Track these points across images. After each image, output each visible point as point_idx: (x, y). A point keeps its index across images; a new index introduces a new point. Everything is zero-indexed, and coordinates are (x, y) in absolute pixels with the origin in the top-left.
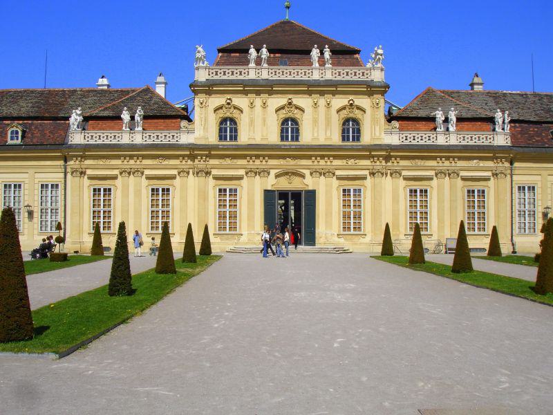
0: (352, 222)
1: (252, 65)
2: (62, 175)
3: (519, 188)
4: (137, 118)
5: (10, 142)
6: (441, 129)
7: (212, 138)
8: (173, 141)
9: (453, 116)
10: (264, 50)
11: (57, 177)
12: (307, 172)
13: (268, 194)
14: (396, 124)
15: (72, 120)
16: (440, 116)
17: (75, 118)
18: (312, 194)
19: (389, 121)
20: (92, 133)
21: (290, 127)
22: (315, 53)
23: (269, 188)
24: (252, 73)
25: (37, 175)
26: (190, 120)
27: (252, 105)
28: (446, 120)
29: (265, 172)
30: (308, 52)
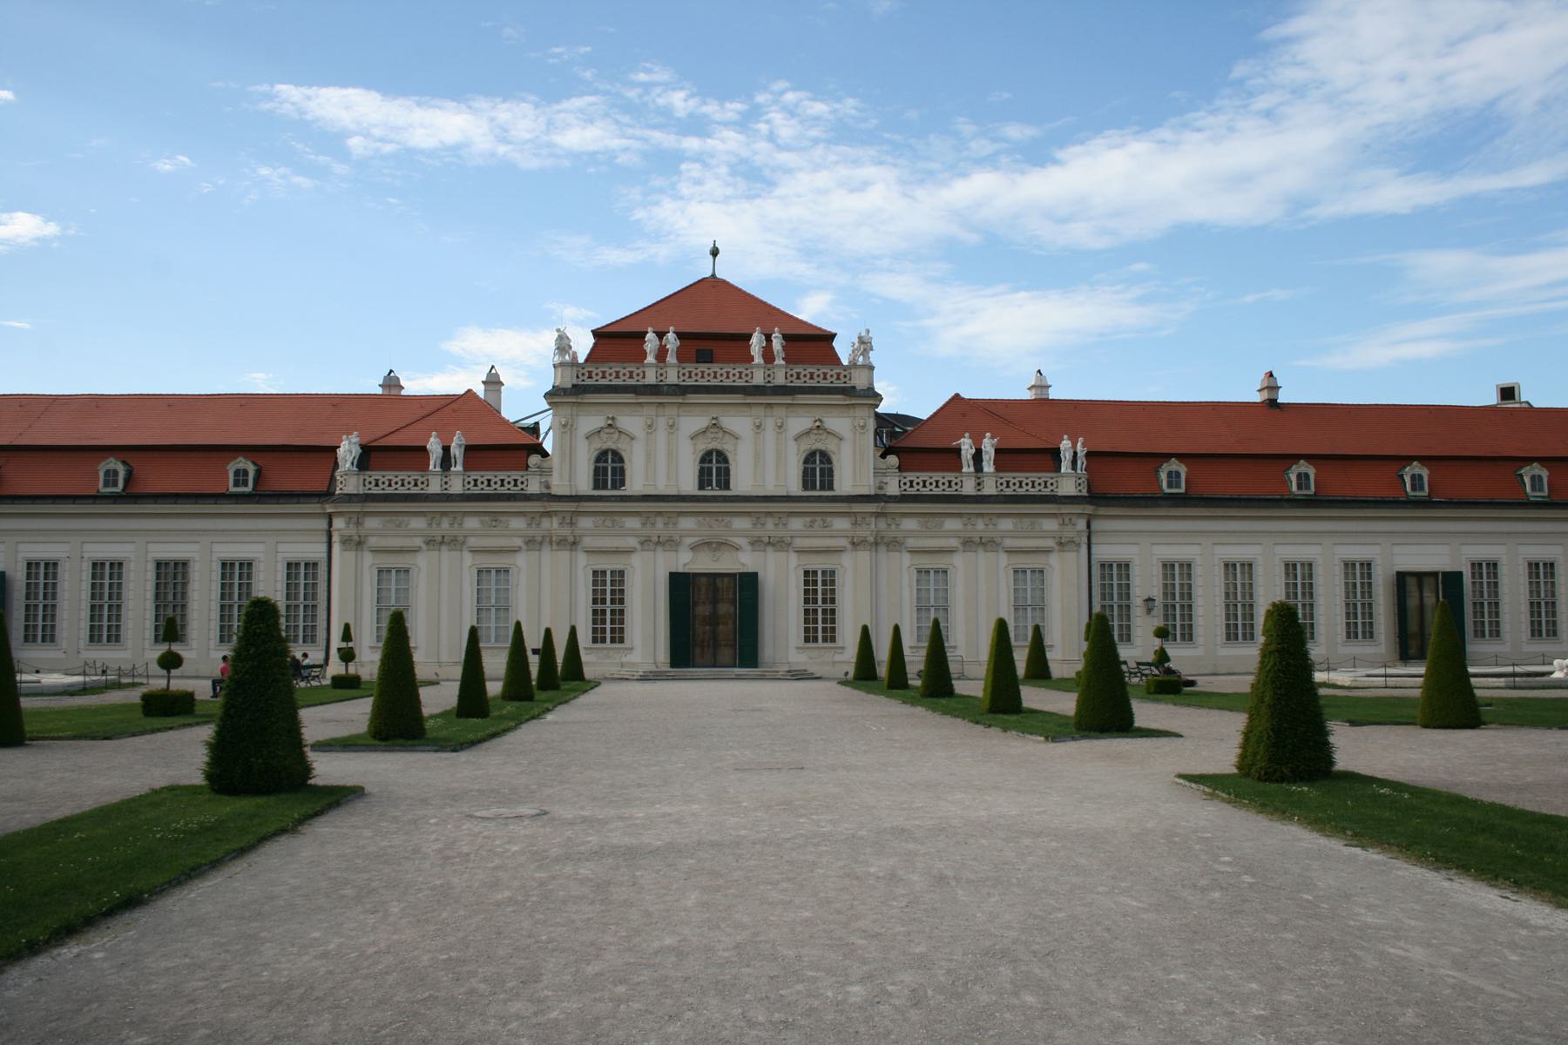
0: (820, 621)
2: (324, 547)
3: (1103, 566)
5: (233, 489)
6: (968, 468)
9: (988, 445)
11: (316, 551)
13: (680, 584)
14: (893, 460)
15: (341, 452)
16: (966, 446)
17: (348, 451)
18: (748, 583)
19: (883, 456)
20: (376, 475)
21: (714, 467)
23: (681, 570)
25: (281, 547)
28: (978, 457)
29: (670, 544)
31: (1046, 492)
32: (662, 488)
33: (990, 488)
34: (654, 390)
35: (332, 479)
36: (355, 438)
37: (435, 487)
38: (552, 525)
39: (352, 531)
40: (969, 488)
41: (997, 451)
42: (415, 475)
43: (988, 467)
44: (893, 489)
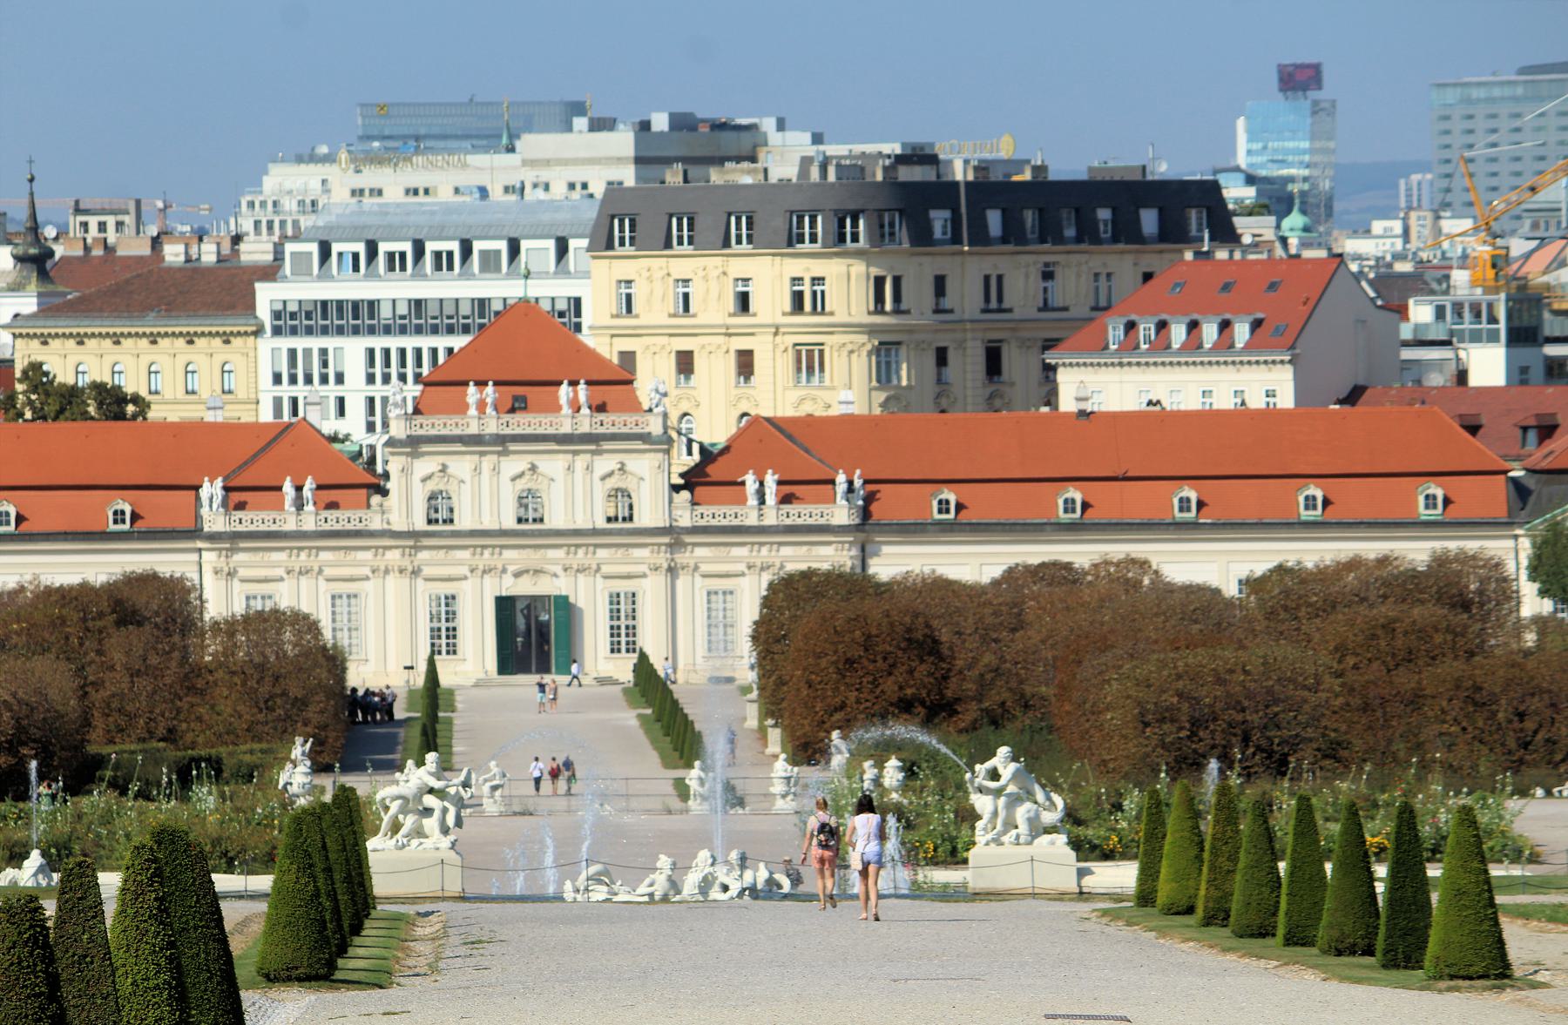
0: (623, 636)
1: (473, 411)
4: (307, 492)
6: (752, 501)
7: (420, 524)
8: (360, 527)
9: (770, 480)
10: (490, 389)
12: (558, 569)
13: (505, 606)
15: (205, 492)
16: (750, 480)
17: (211, 490)
22: (564, 391)
24: (472, 425)
26: (384, 493)
27: (477, 470)
30: (560, 383)
31: (822, 521)
32: (488, 523)
33: (771, 519)
34: (476, 440)
35: (198, 517)
36: (219, 483)
37: (290, 525)
38: (393, 556)
39: (222, 562)
40: (752, 520)
41: (780, 483)
42: (274, 514)
43: (771, 499)
44: (685, 519)
